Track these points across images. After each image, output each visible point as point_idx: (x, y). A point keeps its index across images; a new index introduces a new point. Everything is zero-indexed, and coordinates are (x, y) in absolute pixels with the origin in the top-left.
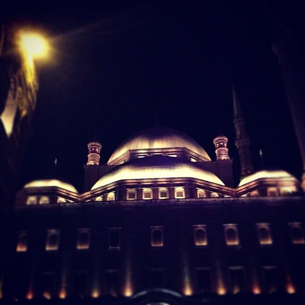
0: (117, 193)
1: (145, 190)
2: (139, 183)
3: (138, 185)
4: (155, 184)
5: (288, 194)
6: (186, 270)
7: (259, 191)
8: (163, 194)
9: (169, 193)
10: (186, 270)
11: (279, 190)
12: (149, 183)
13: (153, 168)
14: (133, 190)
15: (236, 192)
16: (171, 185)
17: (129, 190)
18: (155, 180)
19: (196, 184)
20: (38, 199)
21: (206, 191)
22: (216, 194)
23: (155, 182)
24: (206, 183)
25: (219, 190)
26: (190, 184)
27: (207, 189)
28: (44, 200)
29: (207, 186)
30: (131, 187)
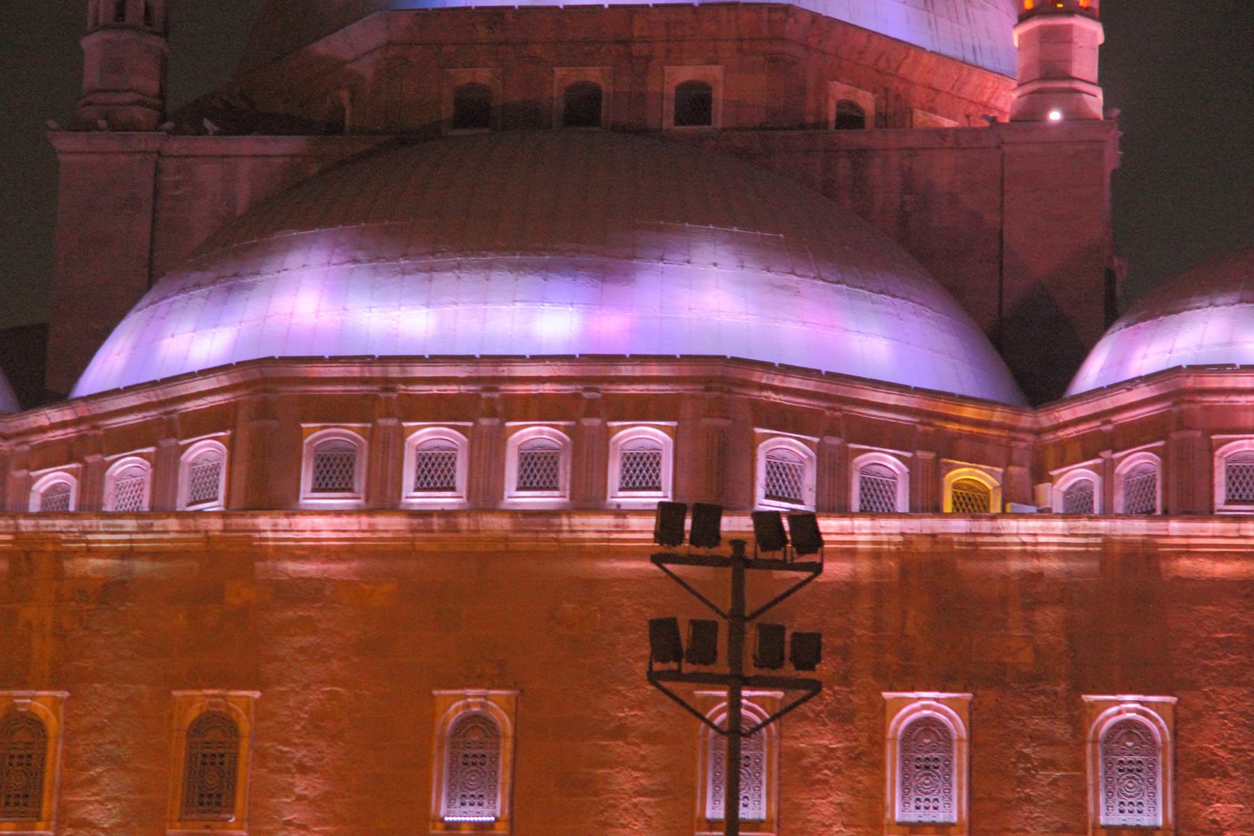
0: (242, 446)
1: (424, 435)
2: (388, 384)
7: (1162, 453)
8: (537, 471)
9: (576, 454)
12: (452, 389)
13: (489, 266)
14: (347, 433)
15: (1039, 432)
16: (592, 411)
17: (316, 434)
18: (486, 371)
19: (755, 404)
21: (819, 449)
22: (889, 461)
23: (493, 382)
24: (824, 388)
27: (834, 432)
29: (834, 411)
30: (333, 411)
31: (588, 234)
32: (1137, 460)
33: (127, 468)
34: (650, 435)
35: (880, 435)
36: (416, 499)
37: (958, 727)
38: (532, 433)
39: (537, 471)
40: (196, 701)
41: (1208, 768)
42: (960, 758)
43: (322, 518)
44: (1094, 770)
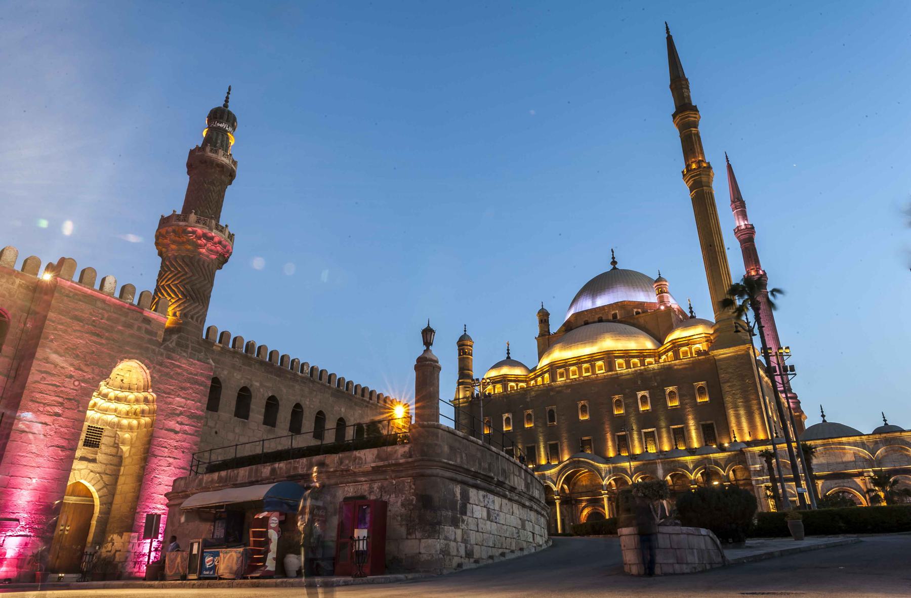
1: (572, 368)
3: (565, 365)
4: (579, 362)
5: (699, 353)
6: (609, 436)
8: (587, 370)
10: (609, 436)
11: (690, 349)
14: (562, 370)
17: (559, 371)
20: (494, 387)
22: (636, 360)
25: (642, 355)
26: (609, 357)
28: (499, 389)
29: (627, 355)
30: (560, 367)
31: (592, 339)
32: (670, 353)
33: (539, 379)
34: (600, 363)
35: (634, 357)
36: (572, 377)
37: (648, 396)
38: (585, 365)
39: (587, 370)
40: (548, 409)
41: (684, 395)
42: (649, 400)
43: (560, 380)
44: (668, 399)
